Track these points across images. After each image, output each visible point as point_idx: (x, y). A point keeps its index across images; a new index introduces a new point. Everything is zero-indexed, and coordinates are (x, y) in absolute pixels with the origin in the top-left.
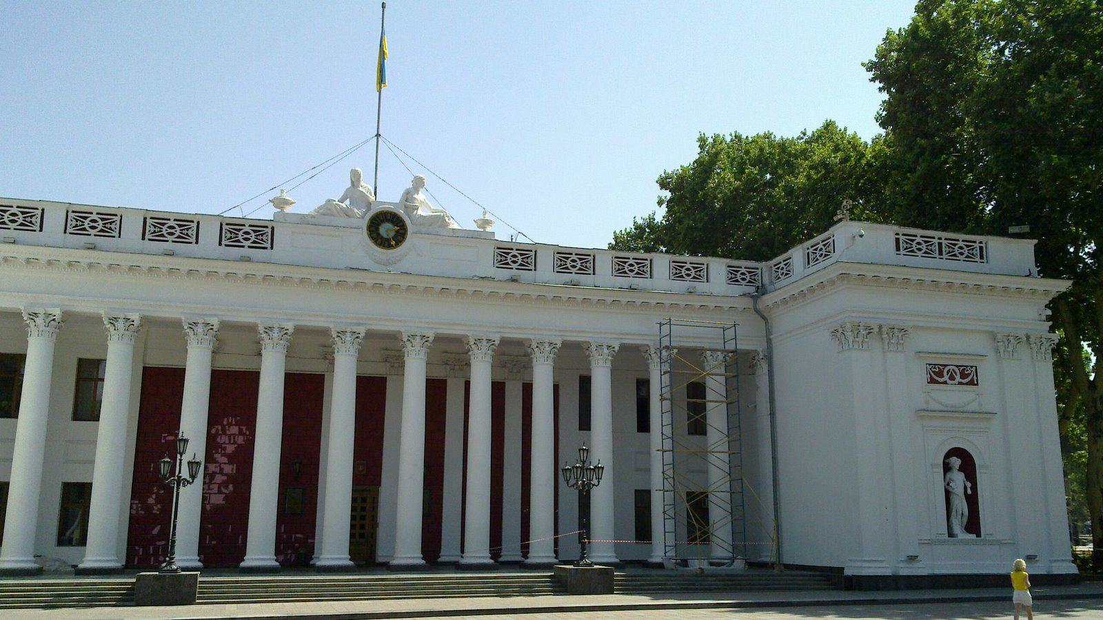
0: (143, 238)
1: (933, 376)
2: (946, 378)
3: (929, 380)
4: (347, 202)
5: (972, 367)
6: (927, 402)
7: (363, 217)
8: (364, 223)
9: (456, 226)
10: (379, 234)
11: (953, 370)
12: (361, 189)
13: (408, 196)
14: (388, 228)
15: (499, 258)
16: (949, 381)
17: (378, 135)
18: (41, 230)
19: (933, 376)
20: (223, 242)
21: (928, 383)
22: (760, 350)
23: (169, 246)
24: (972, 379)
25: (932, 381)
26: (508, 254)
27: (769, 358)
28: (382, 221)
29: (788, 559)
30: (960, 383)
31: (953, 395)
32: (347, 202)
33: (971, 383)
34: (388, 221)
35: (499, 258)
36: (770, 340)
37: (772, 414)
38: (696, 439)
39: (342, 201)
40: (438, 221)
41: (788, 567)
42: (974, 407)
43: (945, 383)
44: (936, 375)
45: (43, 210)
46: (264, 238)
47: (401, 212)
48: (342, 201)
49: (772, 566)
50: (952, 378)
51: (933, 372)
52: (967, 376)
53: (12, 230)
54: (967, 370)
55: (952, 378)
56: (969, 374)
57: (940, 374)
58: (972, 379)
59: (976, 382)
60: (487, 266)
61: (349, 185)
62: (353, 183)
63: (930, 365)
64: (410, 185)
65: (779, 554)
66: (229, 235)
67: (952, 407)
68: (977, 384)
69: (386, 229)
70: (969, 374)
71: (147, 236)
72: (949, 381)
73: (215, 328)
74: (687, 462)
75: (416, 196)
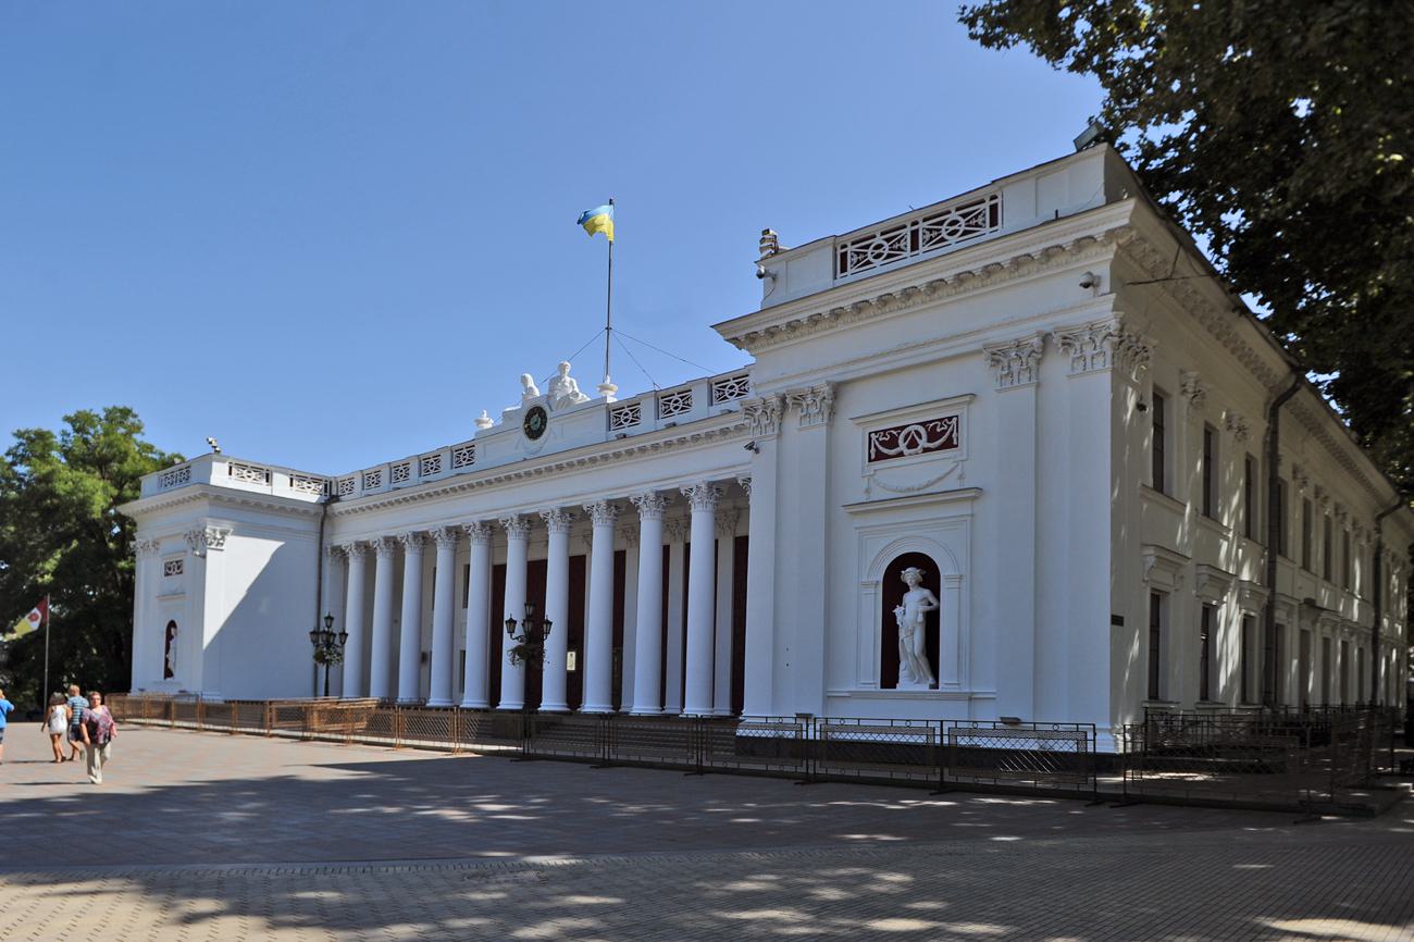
1: (881, 448)
2: (902, 446)
3: (873, 457)
5: (950, 419)
6: (868, 491)
8: (520, 422)
11: (916, 431)
16: (906, 452)
19: (881, 448)
21: (870, 460)
24: (950, 438)
25: (880, 456)
30: (926, 450)
31: (915, 470)
33: (949, 444)
42: (951, 483)
43: (901, 454)
44: (885, 445)
50: (913, 444)
51: (882, 443)
52: (941, 435)
54: (942, 426)
55: (913, 444)
56: (944, 432)
57: (893, 443)
58: (950, 438)
59: (955, 443)
60: (596, 429)
63: (876, 433)
67: (909, 489)
68: (957, 446)
70: (944, 432)
72: (906, 452)
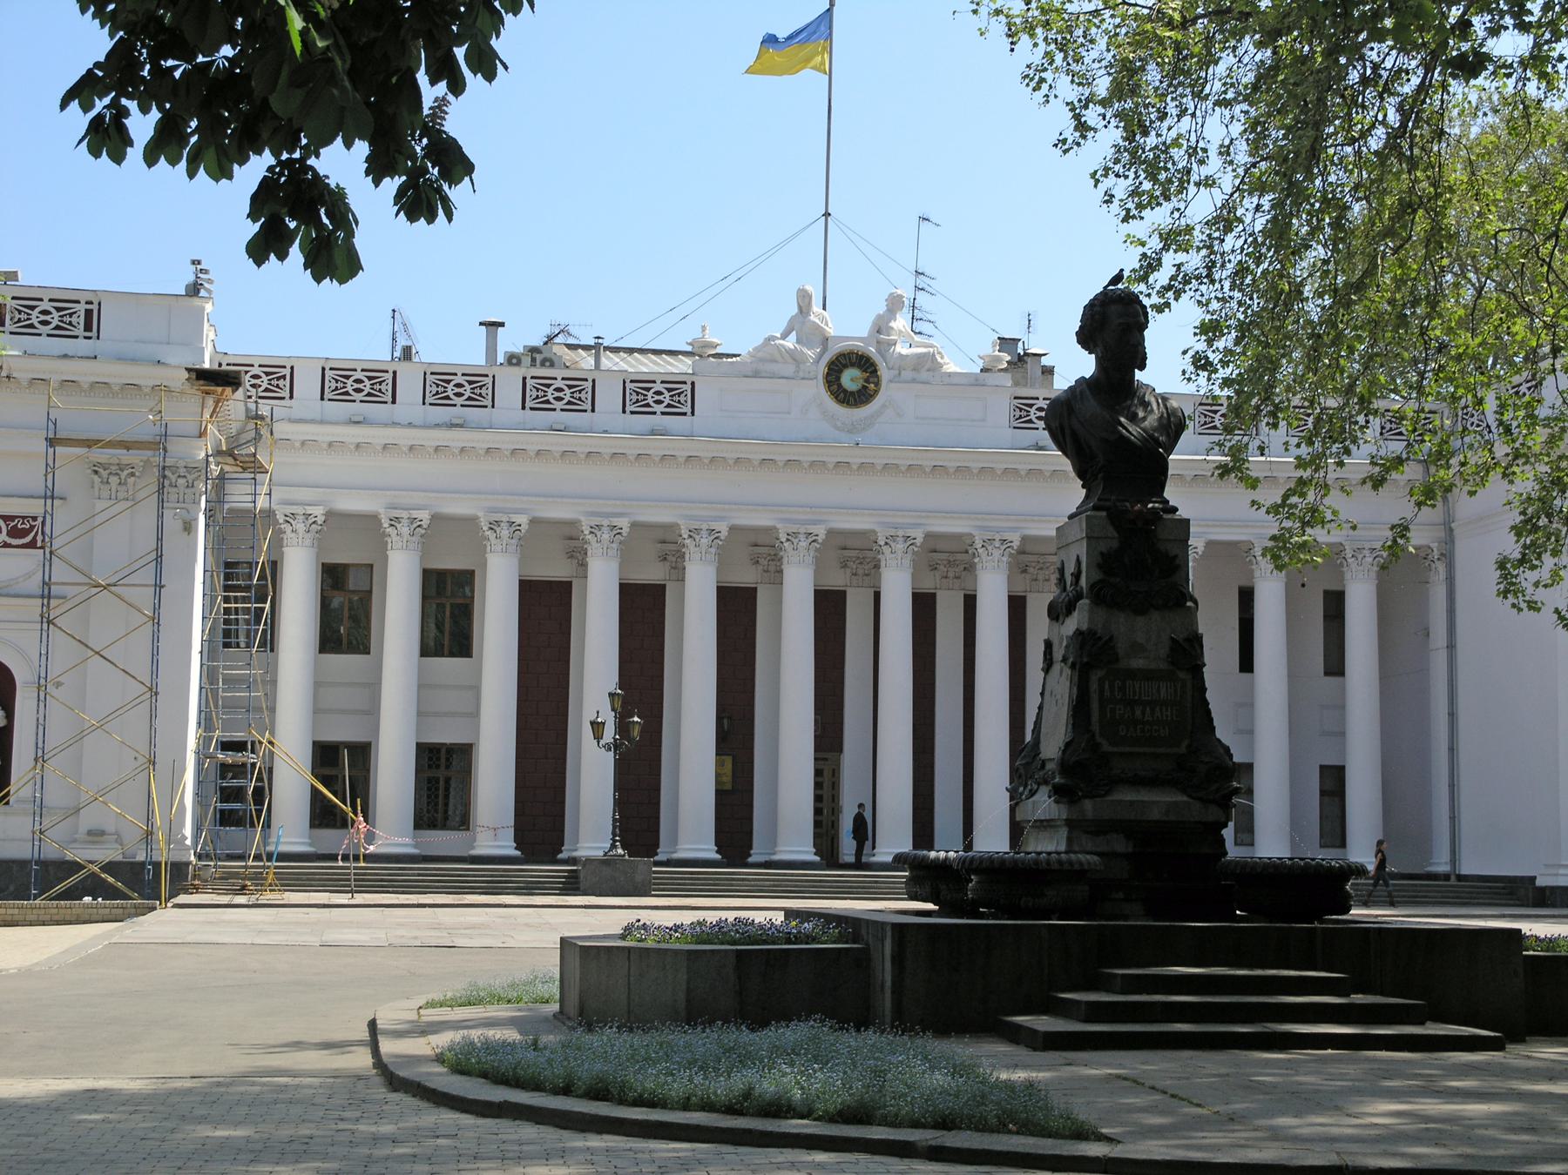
0: (524, 408)
4: (793, 336)
7: (817, 361)
8: (822, 369)
9: (951, 367)
10: (840, 386)
12: (812, 318)
13: (881, 327)
14: (853, 376)
15: (1018, 413)
17: (827, 214)
18: (394, 402)
20: (628, 409)
22: (1434, 545)
23: (559, 417)
26: (1031, 406)
27: (1448, 557)
28: (845, 366)
29: (1466, 869)
32: (793, 336)
34: (853, 365)
35: (1018, 413)
36: (1451, 530)
37: (1451, 646)
38: (1333, 681)
39: (784, 336)
40: (926, 365)
41: (1460, 878)
45: (395, 373)
46: (682, 399)
47: (872, 350)
48: (784, 336)
49: (1447, 877)
53: (357, 404)
61: (795, 310)
62: (800, 308)
64: (882, 308)
65: (1454, 861)
66: (635, 397)
69: (851, 379)
71: (529, 404)
73: (625, 531)
74: (1314, 718)
75: (892, 324)
